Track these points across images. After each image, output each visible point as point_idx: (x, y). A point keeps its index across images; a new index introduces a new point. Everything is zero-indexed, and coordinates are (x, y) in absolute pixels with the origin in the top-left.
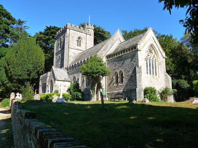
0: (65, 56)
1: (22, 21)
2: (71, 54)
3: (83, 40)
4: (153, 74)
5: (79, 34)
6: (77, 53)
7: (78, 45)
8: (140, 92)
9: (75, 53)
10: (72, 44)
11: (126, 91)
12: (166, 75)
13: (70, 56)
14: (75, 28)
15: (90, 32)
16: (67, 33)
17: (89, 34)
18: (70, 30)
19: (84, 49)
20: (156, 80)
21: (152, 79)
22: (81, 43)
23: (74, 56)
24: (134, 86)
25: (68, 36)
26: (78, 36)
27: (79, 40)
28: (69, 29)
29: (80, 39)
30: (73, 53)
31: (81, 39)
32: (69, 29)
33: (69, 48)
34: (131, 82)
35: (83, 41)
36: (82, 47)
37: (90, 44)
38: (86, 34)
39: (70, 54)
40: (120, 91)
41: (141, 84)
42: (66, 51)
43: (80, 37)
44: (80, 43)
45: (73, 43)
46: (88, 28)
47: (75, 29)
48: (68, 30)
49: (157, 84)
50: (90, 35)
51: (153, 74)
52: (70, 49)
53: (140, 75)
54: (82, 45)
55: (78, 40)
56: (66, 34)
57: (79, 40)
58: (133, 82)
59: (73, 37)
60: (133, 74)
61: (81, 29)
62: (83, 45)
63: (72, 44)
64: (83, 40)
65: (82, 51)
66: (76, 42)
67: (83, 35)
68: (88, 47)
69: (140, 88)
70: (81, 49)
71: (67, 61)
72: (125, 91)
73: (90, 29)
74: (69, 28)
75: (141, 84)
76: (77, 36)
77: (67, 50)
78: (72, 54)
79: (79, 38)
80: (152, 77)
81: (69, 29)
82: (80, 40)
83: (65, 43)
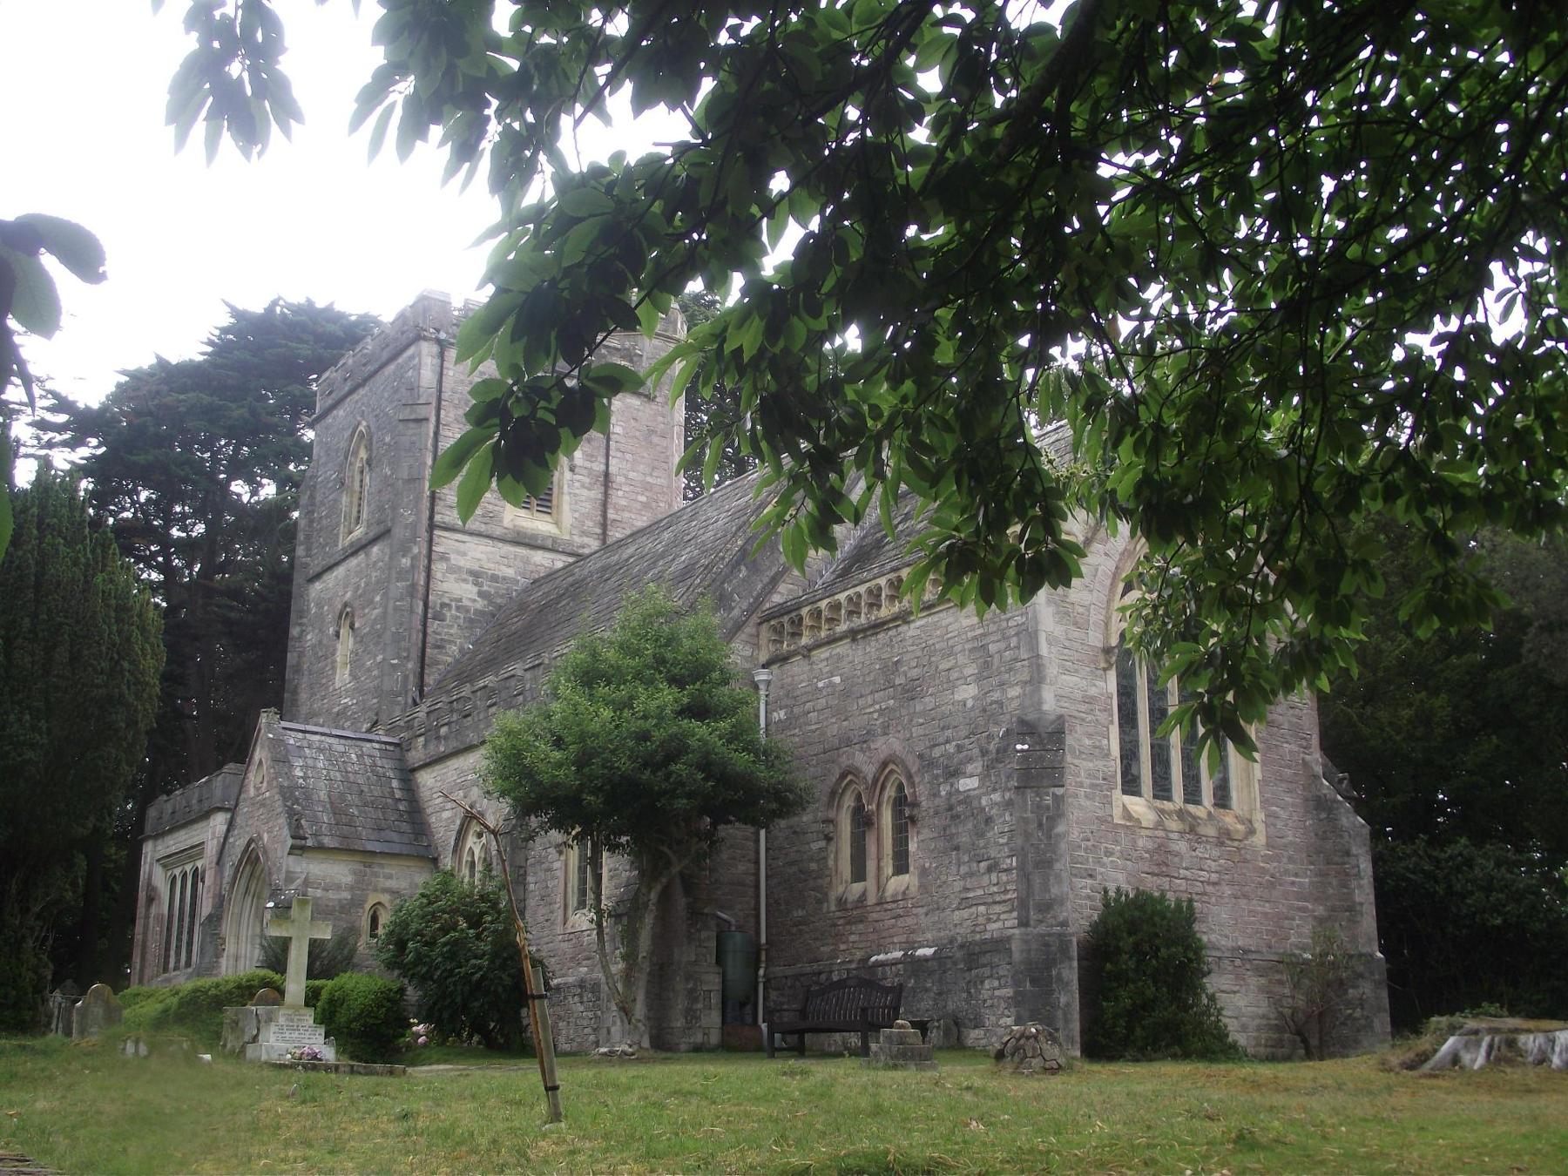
4: (1193, 795)
6: (510, 572)
8: (1049, 963)
9: (494, 578)
11: (929, 951)
12: (1320, 805)
13: (443, 605)
20: (1215, 853)
21: (1181, 846)
23: (481, 604)
24: (997, 909)
28: (435, 349)
30: (476, 576)
32: (439, 341)
33: (432, 526)
34: (971, 874)
37: (647, 487)
39: (445, 586)
40: (882, 957)
41: (1055, 891)
49: (1228, 891)
51: (1193, 795)
52: (445, 542)
53: (1048, 808)
54: (566, 498)
58: (989, 870)
60: (996, 797)
65: (560, 562)
68: (630, 515)
69: (1042, 929)
70: (555, 540)
71: (415, 654)
72: (920, 952)
74: (443, 336)
75: (1055, 891)
77: (419, 549)
78: (466, 592)
80: (1174, 824)
81: (439, 341)
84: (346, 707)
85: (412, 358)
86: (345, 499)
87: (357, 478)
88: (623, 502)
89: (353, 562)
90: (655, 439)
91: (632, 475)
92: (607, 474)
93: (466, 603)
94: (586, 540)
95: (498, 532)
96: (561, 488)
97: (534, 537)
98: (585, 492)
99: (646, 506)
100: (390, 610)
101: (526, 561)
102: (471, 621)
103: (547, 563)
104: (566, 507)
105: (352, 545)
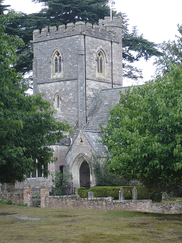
0: (81, 98)
6: (97, 88)
9: (95, 90)
17: (116, 41)
18: (86, 37)
28: (83, 36)
29: (101, 56)
30: (92, 89)
31: (102, 54)
35: (108, 60)
38: (112, 42)
45: (90, 66)
46: (112, 25)
50: (118, 43)
76: (97, 50)
77: (84, 85)
79: (99, 55)
85: (78, 38)
86: (52, 67)
87: (54, 61)
89: (58, 83)
92: (112, 63)
96: (104, 67)
97: (101, 80)
98: (108, 68)
99: (118, 69)
100: (79, 99)
102: (92, 100)
105: (57, 79)
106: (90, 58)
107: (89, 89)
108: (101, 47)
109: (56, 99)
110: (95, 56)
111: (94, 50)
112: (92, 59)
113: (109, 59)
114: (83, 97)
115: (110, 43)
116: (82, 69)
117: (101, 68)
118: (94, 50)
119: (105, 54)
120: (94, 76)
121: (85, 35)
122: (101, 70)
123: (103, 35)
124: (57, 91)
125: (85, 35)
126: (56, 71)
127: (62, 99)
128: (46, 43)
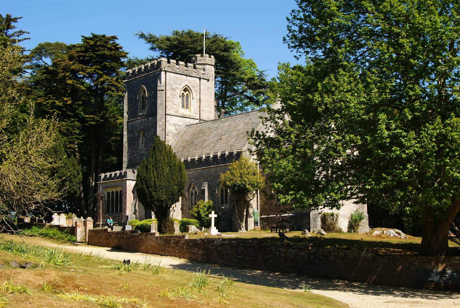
1: (13, 17)
2: (170, 128)
3: (192, 94)
5: (186, 81)
6: (181, 124)
7: (183, 107)
9: (178, 125)
10: (172, 105)
14: (177, 67)
15: (208, 74)
16: (160, 82)
17: (205, 78)
18: (167, 73)
19: (194, 115)
22: (189, 99)
23: (176, 131)
25: (163, 88)
26: (184, 84)
27: (185, 94)
29: (187, 92)
30: (174, 125)
33: (166, 114)
35: (194, 96)
36: (192, 110)
37: (208, 101)
38: (200, 79)
42: (161, 123)
43: (186, 88)
44: (187, 100)
46: (202, 62)
47: (178, 70)
48: (163, 73)
50: (208, 80)
52: (168, 118)
54: (192, 105)
55: (183, 94)
56: (159, 83)
57: (185, 94)
59: (174, 90)
61: (189, 69)
62: (194, 104)
63: (172, 105)
64: (194, 95)
66: (180, 100)
67: (192, 82)
73: (207, 67)
74: (166, 70)
76: (182, 86)
77: (164, 120)
79: (185, 90)
82: (187, 94)
83: (158, 105)
84: (143, 153)
86: (139, 104)
88: (203, 105)
90: (210, 90)
91: (205, 99)
92: (200, 99)
93: (173, 131)
94: (196, 115)
95: (178, 115)
97: (186, 115)
99: (208, 106)
101: (184, 121)
103: (188, 121)
104: (192, 108)
106: (172, 94)
107: (170, 124)
108: (187, 83)
109: (141, 136)
110: (179, 92)
111: (178, 86)
112: (175, 95)
113: (196, 95)
114: (162, 132)
115: (198, 80)
116: (161, 104)
117: (187, 104)
118: (178, 86)
119: (191, 90)
120: (177, 111)
121: (166, 72)
122: (186, 105)
123: (189, 72)
124: (142, 127)
125: (166, 72)
126: (142, 109)
127: (146, 135)
128: (135, 82)
